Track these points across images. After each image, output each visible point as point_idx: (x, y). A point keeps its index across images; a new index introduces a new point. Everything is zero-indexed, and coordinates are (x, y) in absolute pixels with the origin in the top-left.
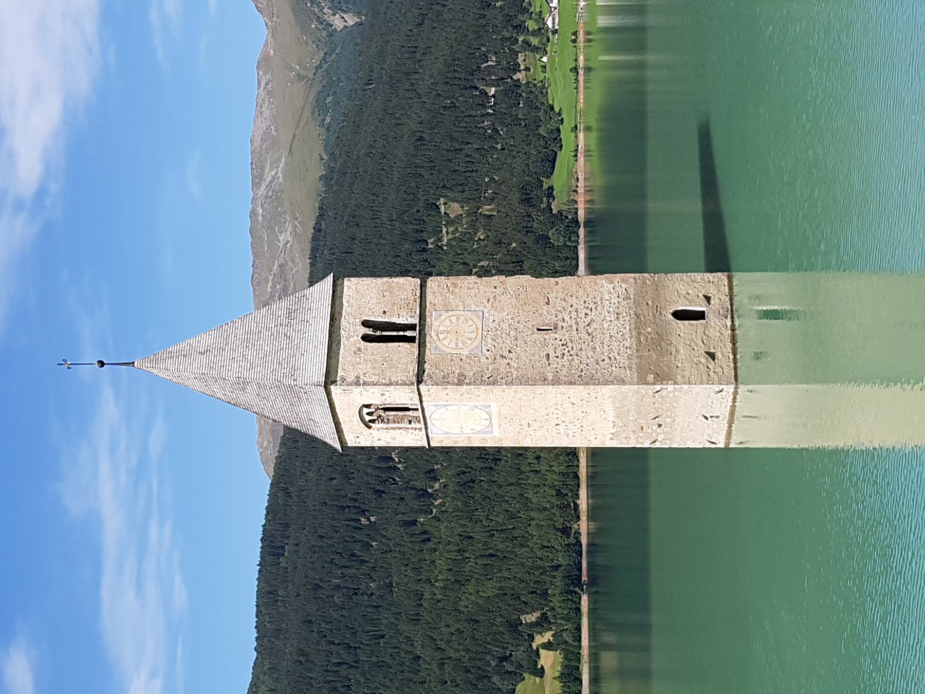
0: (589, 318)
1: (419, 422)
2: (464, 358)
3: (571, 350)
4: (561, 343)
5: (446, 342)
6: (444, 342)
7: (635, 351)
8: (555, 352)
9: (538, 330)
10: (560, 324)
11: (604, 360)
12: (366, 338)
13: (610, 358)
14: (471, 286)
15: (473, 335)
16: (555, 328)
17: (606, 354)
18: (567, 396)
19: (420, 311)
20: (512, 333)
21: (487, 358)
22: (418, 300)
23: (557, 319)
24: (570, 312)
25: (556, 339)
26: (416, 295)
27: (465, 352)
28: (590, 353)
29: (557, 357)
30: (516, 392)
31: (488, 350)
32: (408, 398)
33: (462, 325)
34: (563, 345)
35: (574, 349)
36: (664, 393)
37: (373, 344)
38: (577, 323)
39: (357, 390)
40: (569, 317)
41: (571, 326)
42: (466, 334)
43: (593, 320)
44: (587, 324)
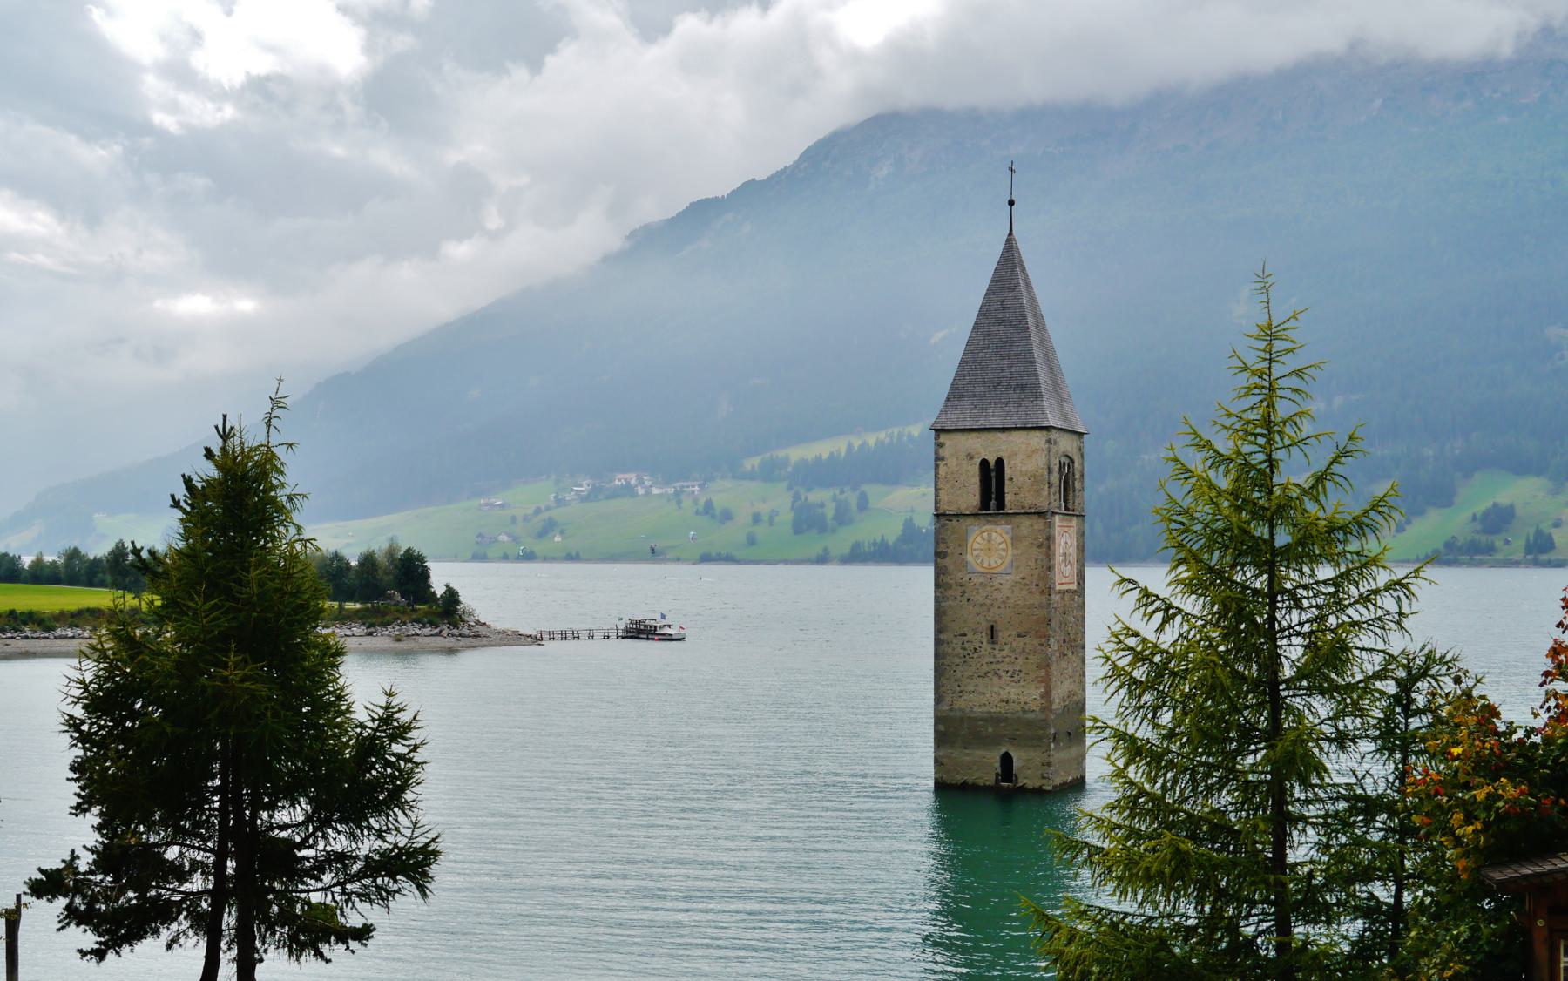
0: (1003, 674)
5: (979, 539)
9: (992, 627)
10: (997, 647)
12: (984, 463)
13: (961, 692)
15: (986, 565)
16: (993, 643)
20: (988, 602)
27: (969, 558)
34: (975, 649)
41: (994, 657)
43: (1000, 677)
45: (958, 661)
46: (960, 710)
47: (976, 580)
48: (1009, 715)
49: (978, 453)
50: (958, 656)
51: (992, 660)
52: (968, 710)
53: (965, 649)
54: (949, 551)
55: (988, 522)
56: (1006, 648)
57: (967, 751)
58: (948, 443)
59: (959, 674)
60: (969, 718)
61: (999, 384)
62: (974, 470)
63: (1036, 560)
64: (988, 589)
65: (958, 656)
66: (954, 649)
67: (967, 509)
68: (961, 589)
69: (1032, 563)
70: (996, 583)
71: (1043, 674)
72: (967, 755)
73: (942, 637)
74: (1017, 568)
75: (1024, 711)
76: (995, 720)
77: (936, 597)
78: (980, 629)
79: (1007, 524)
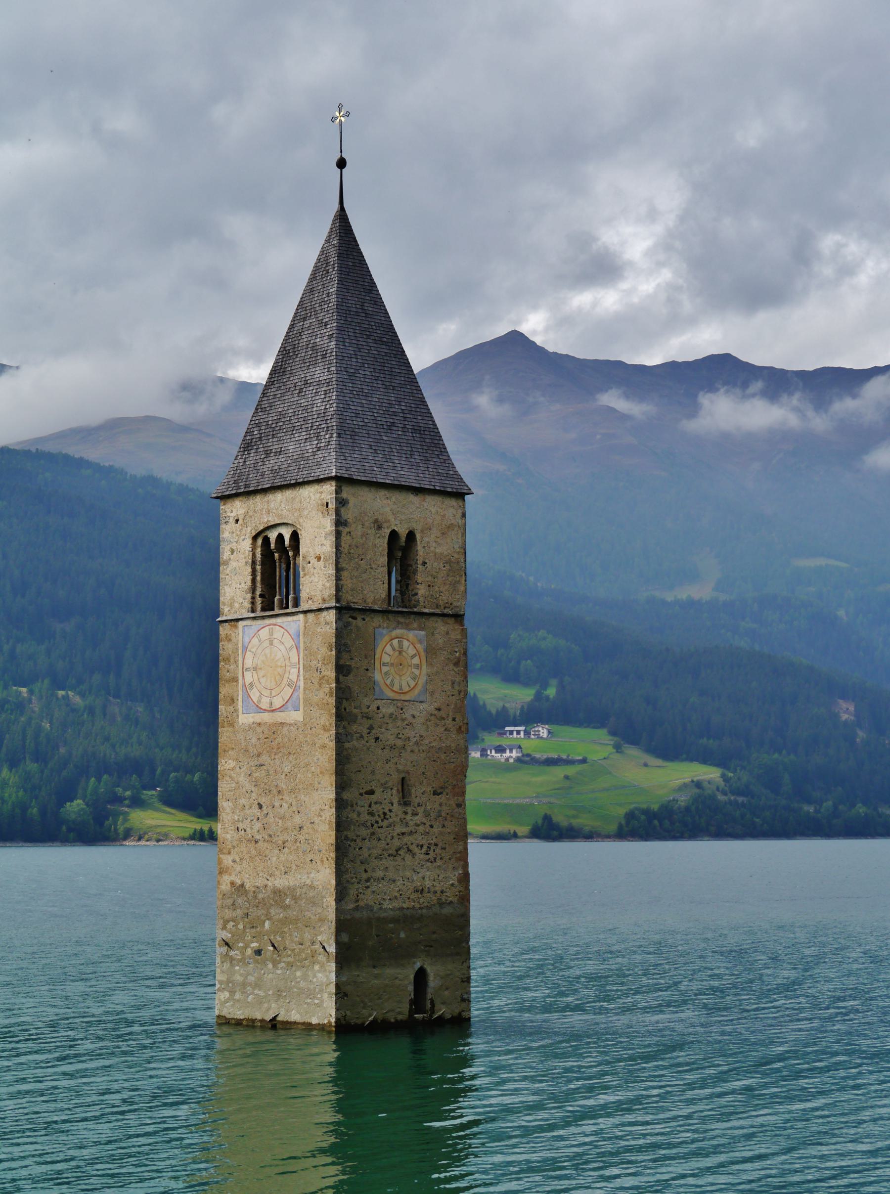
0: (416, 850)
1: (281, 608)
2: (369, 674)
3: (379, 825)
4: (386, 811)
5: (388, 649)
6: (388, 645)
7: (376, 915)
8: (376, 803)
9: (403, 779)
10: (409, 810)
11: (366, 871)
13: (368, 880)
14: (456, 687)
17: (374, 875)
18: (316, 819)
19: (426, 614)
20: (399, 743)
21: (368, 707)
22: (438, 611)
23: (416, 805)
24: (425, 824)
25: (392, 805)
26: (445, 608)
27: (378, 677)
28: (375, 852)
29: (370, 806)
30: (324, 747)
31: (378, 708)
32: (313, 593)
33: (408, 673)
34: (385, 814)
35: (380, 830)
36: (322, 958)
37: (386, 546)
38: (411, 833)
39: (328, 524)
40: (418, 822)
41: (407, 825)
42: (398, 677)
43: (414, 855)
44: (411, 847)
45: (364, 832)
46: (369, 908)
47: (387, 710)
48: (424, 911)
49: (389, 521)
50: (364, 824)
51: (404, 830)
52: (376, 908)
53: (371, 814)
54: (353, 665)
55: (399, 623)
56: (420, 810)
57: (376, 971)
58: (352, 501)
59: (365, 853)
60: (378, 919)
61: (393, 424)
62: (383, 543)
63: (453, 683)
64: (399, 723)
65: (364, 824)
66: (359, 814)
67: (375, 602)
68: (367, 723)
69: (447, 687)
70: (407, 715)
71: (461, 848)
72: (376, 977)
73: (346, 796)
74: (432, 693)
75: (441, 904)
76: (406, 919)
77: (338, 734)
78: (390, 784)
79: (421, 629)
